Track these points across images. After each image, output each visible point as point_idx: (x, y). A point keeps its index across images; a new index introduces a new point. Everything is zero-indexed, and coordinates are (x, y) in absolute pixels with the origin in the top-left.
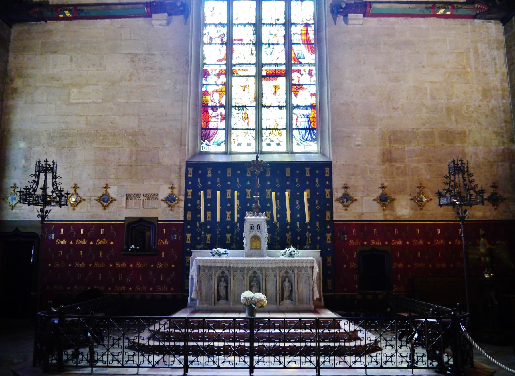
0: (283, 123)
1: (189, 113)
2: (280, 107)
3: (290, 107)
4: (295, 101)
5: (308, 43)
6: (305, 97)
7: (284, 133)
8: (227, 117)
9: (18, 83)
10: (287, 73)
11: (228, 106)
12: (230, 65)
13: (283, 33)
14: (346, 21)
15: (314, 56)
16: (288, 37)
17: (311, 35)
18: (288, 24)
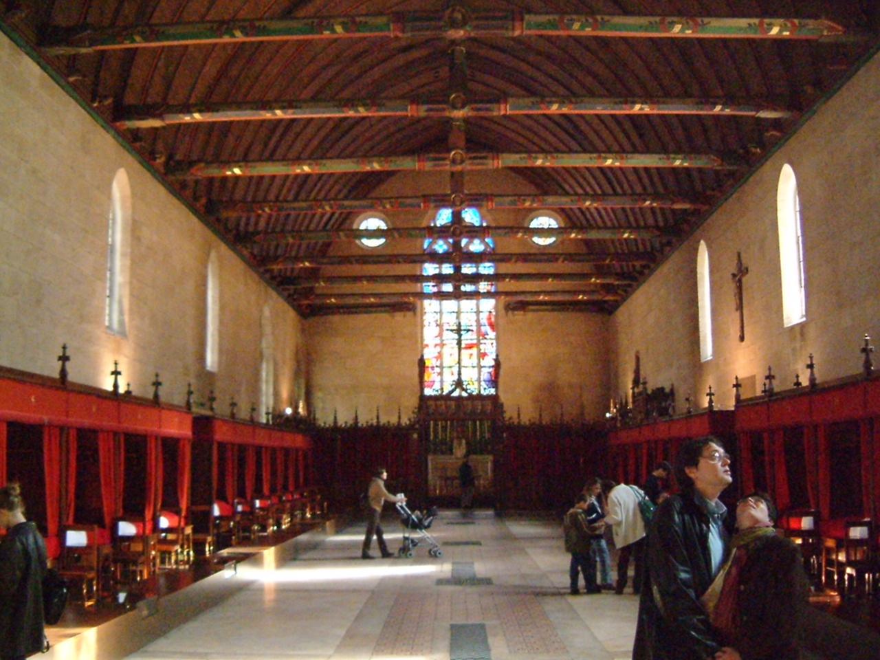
0: (475, 377)
1: (416, 370)
2: (473, 367)
3: (480, 367)
4: (483, 363)
5: (492, 325)
6: (489, 361)
7: (476, 383)
8: (441, 374)
9: (314, 356)
10: (478, 345)
11: (441, 367)
12: (442, 341)
13: (475, 318)
14: (513, 314)
15: (494, 333)
16: (478, 321)
17: (493, 319)
18: (478, 312)
